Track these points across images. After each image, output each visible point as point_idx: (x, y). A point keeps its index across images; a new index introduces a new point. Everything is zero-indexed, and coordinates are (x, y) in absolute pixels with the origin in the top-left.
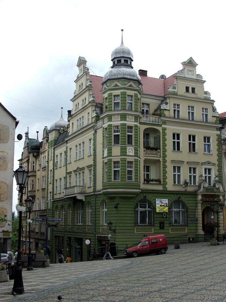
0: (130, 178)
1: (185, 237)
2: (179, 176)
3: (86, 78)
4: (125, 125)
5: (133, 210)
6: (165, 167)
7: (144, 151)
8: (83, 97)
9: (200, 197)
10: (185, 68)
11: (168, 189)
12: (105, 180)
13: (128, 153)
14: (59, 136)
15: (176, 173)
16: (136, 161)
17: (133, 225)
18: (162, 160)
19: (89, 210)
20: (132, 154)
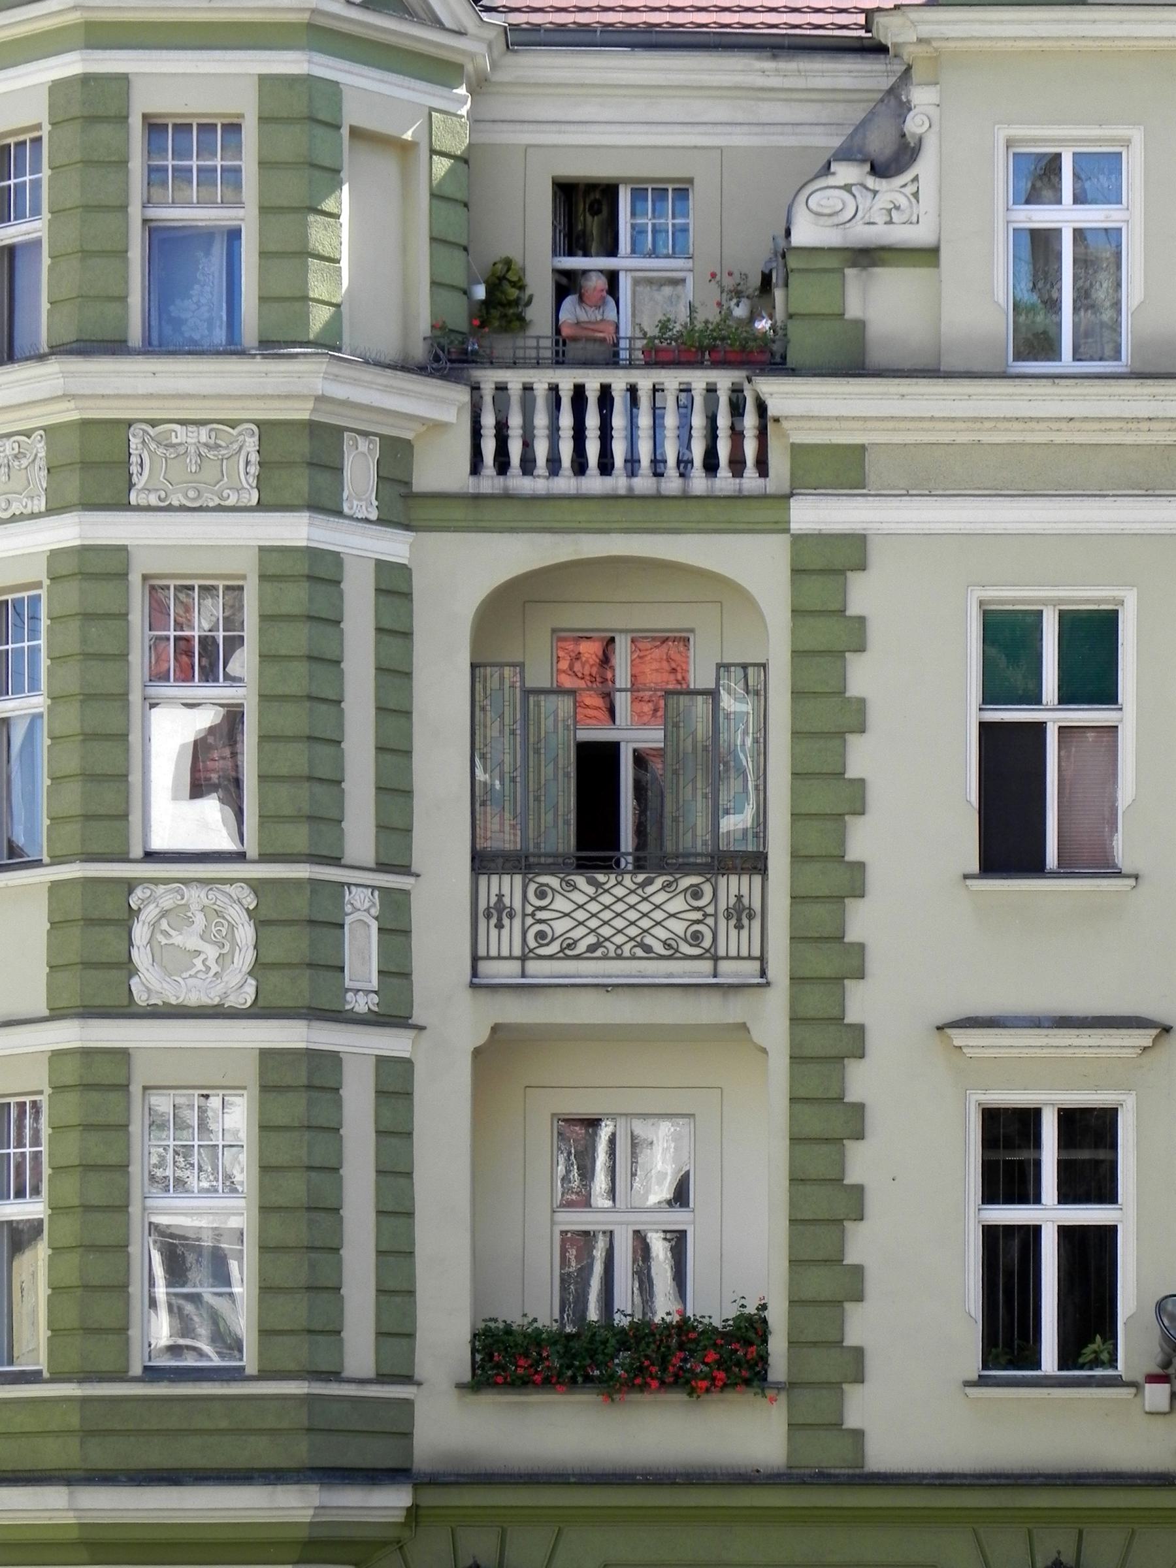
13: (150, 982)
20: (220, 988)
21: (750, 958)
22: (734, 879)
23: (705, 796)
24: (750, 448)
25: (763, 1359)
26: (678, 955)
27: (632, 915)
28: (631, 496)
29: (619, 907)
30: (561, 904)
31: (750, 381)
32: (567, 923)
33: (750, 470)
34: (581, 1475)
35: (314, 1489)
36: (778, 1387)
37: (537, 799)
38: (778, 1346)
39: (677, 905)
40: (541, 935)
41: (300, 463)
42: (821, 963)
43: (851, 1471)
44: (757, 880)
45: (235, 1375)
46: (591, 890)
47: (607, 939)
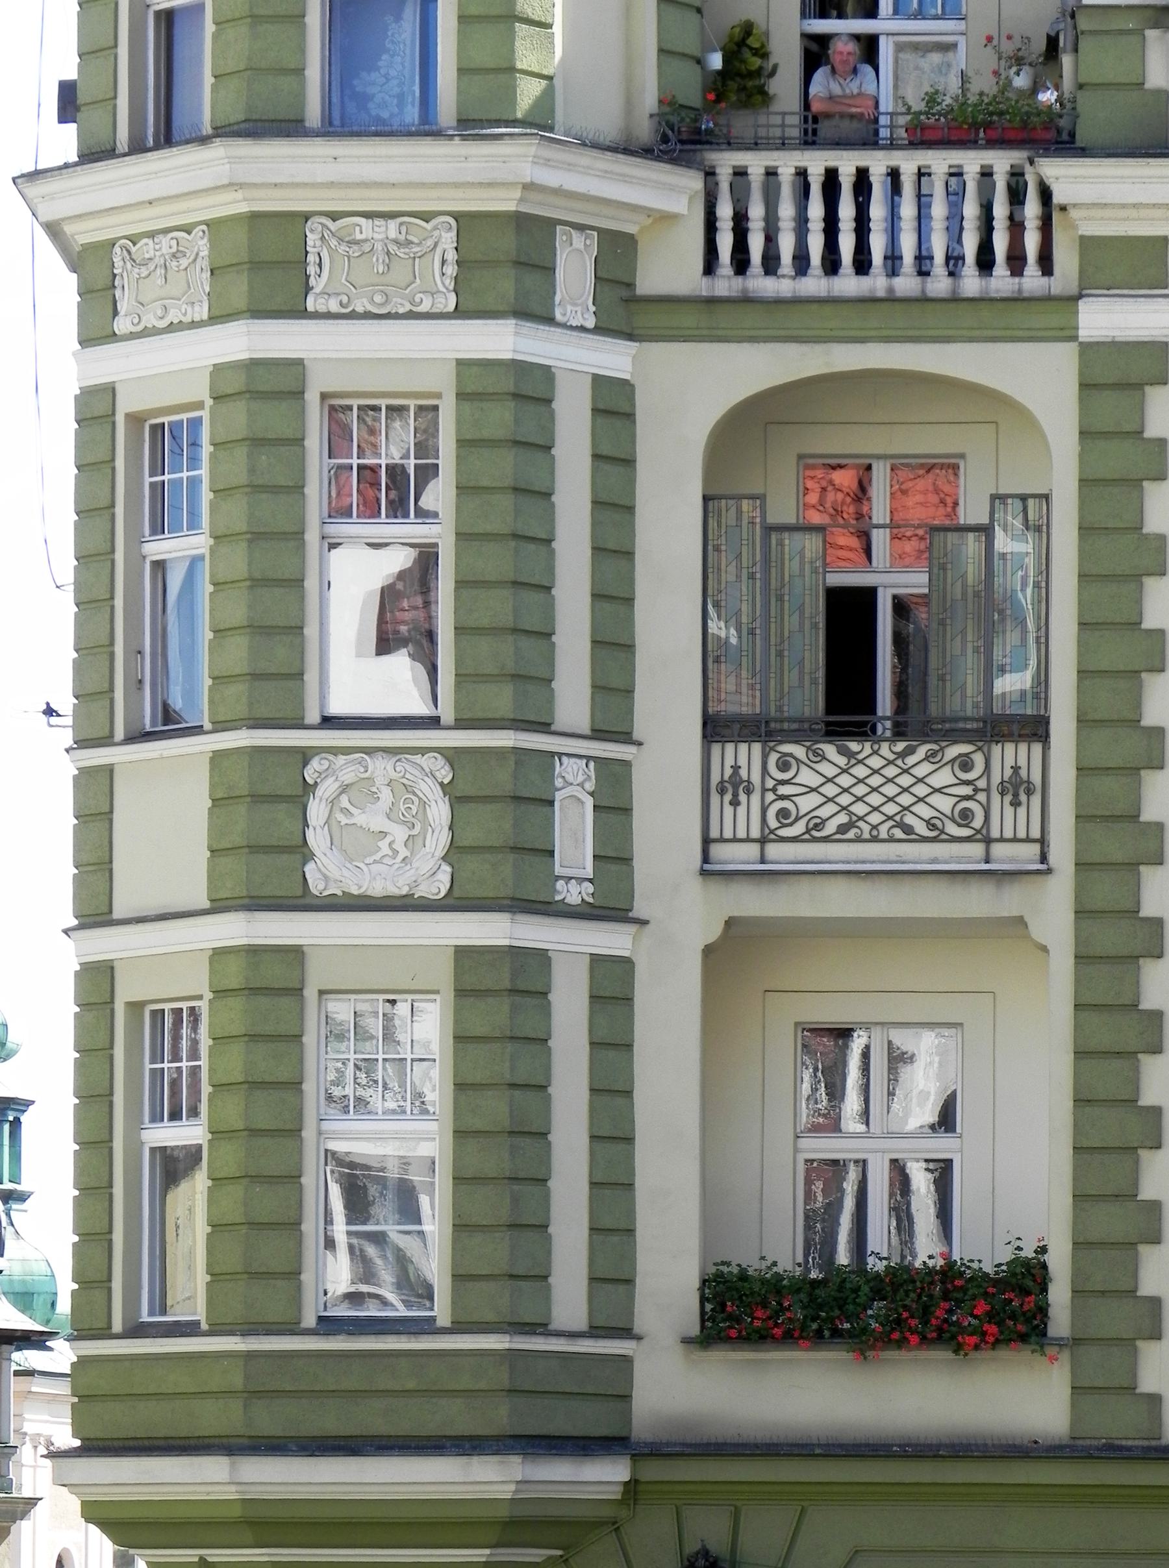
13: (327, 871)
21: (1028, 840)
22: (1010, 748)
23: (976, 650)
24: (1032, 242)
25: (1043, 1311)
26: (944, 837)
27: (890, 790)
28: (891, 299)
29: (875, 781)
30: (807, 777)
31: (1032, 163)
32: (814, 800)
33: (1032, 267)
34: (828, 1445)
35: (516, 1460)
36: (1060, 1343)
37: (780, 654)
38: (1059, 1294)
39: (943, 778)
40: (783, 814)
41: (506, 261)
42: (1112, 846)
43: (1145, 1443)
44: (1037, 748)
45: (425, 1327)
46: (842, 761)
47: (860, 818)
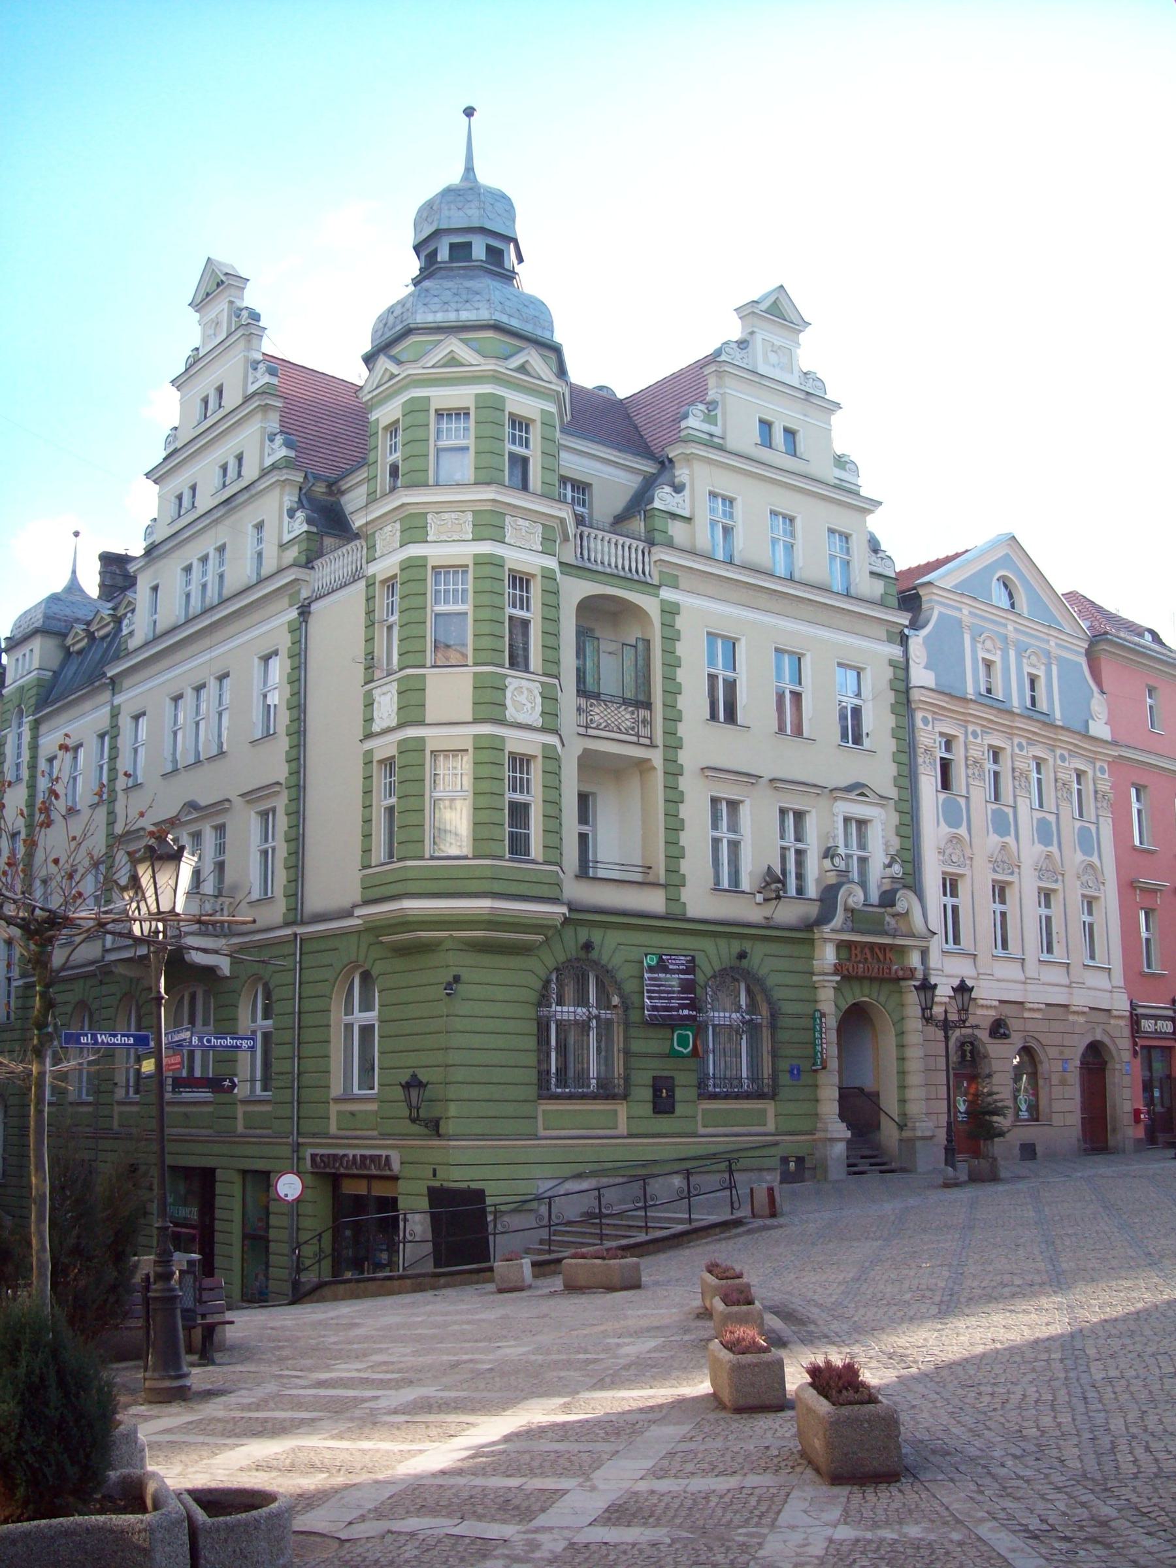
0: (519, 845)
1: (765, 1152)
2: (734, 846)
3: (246, 359)
4: (496, 562)
5: (531, 1012)
6: (674, 798)
7: (579, 709)
8: (225, 451)
9: (828, 955)
10: (752, 333)
11: (692, 912)
12: (379, 853)
13: (511, 713)
14: (63, 665)
15: (724, 833)
16: (551, 756)
17: (532, 1092)
18: (662, 761)
19: (254, 1020)
30: (596, 710)
